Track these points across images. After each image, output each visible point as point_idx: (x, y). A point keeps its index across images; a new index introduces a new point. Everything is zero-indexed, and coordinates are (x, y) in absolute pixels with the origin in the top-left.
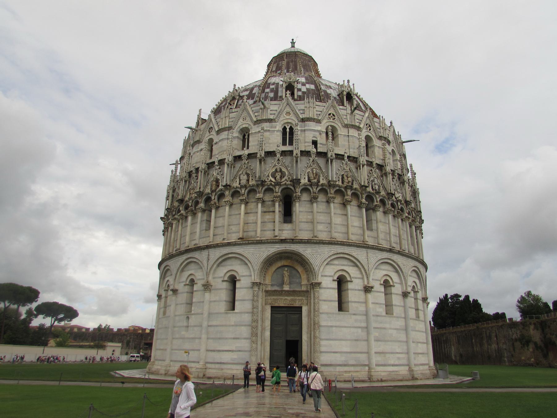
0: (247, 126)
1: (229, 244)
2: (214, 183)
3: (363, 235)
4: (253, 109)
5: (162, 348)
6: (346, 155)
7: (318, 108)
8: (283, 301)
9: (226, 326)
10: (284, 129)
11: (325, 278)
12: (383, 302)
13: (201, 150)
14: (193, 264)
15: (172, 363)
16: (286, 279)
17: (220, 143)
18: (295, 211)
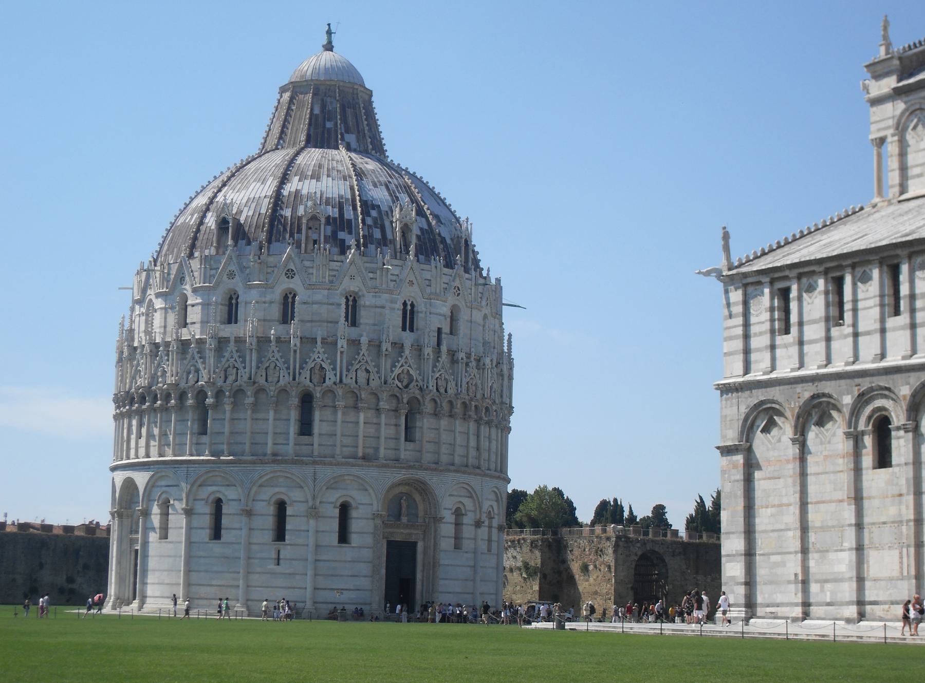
0: (357, 290)
1: (347, 464)
2: (317, 371)
3: (478, 458)
4: (368, 265)
5: (214, 583)
7: (445, 279)
8: (400, 535)
9: (340, 561)
10: (405, 304)
11: (446, 511)
12: (487, 538)
13: (271, 302)
14: (281, 480)
15: (250, 603)
16: (404, 509)
17: (314, 306)
18: (421, 428)
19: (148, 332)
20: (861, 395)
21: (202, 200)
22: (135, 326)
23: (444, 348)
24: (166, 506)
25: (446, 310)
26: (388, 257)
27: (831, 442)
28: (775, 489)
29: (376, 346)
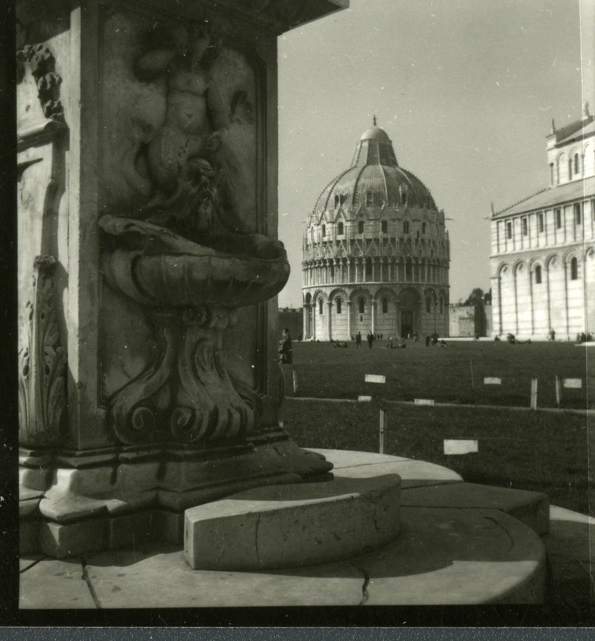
6: (432, 241)
10: (404, 223)
19: (313, 239)
20: (532, 259)
21: (329, 189)
22: (308, 237)
23: (419, 239)
24: (321, 303)
25: (421, 224)
26: (397, 206)
27: (523, 276)
28: (507, 292)
29: (393, 240)
